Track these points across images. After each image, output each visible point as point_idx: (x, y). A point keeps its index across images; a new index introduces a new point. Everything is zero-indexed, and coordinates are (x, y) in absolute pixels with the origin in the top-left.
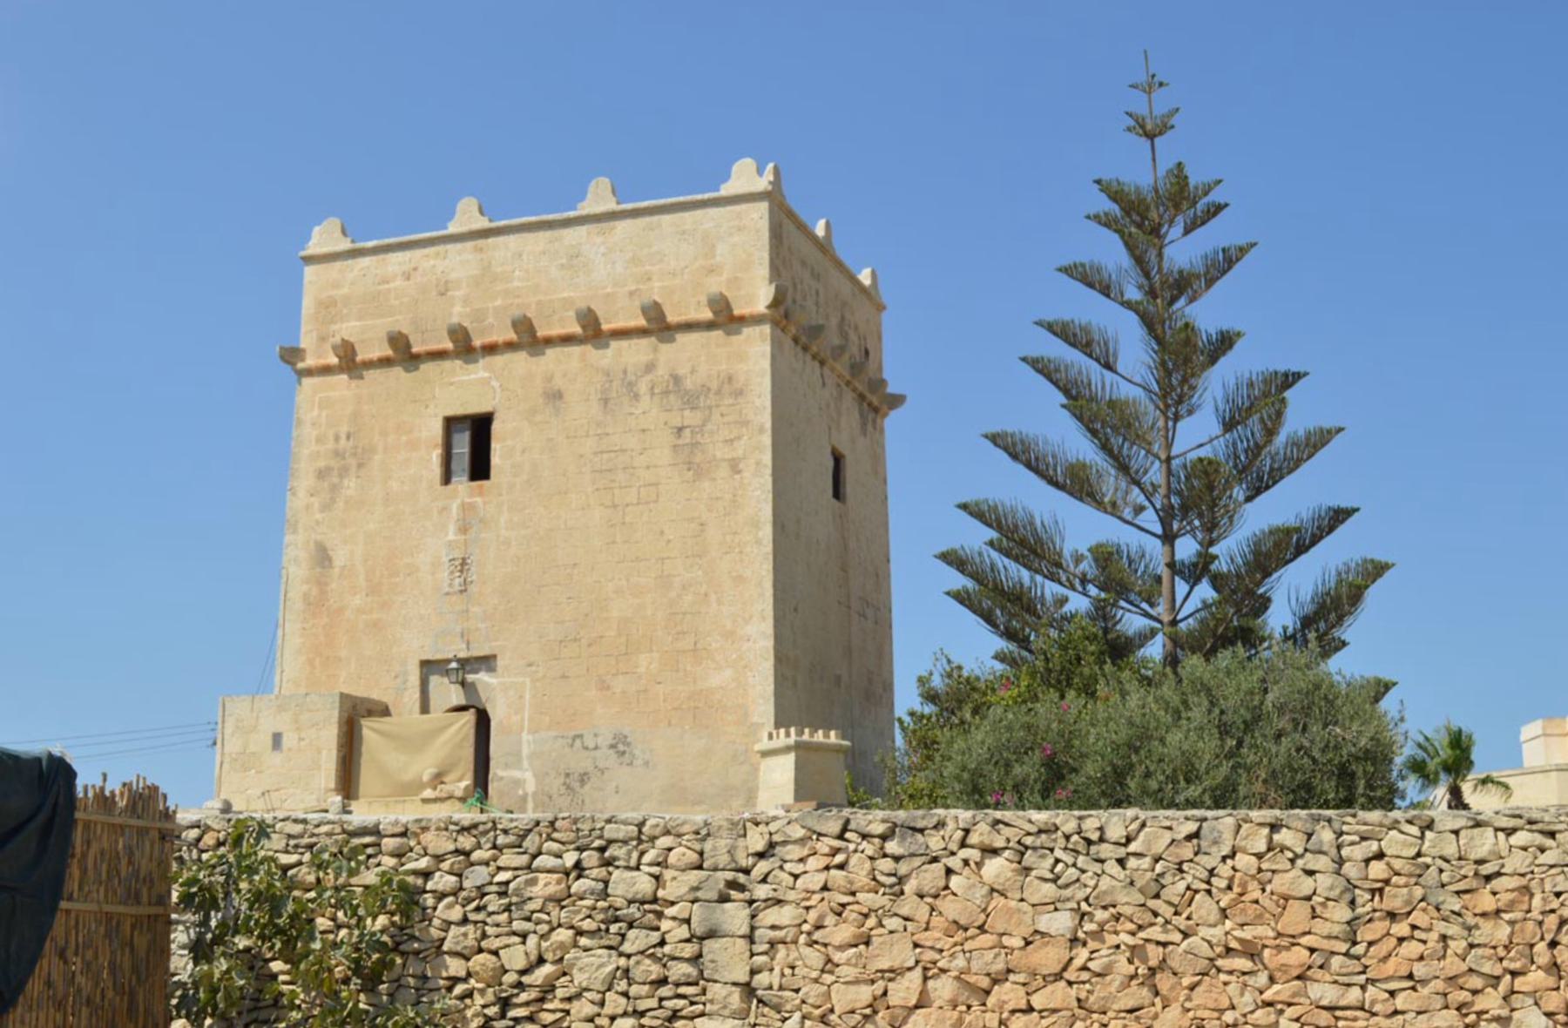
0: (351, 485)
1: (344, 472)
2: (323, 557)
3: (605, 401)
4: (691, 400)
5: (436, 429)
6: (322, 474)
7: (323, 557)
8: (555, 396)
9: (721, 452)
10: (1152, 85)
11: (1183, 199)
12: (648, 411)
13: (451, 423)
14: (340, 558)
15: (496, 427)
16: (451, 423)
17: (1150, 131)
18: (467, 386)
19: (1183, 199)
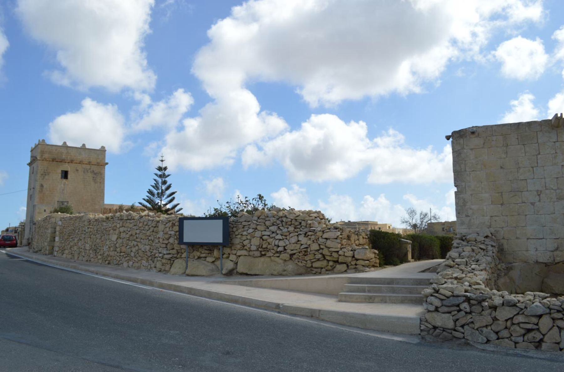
0: (47, 177)
1: (45, 175)
2: (42, 186)
3: (84, 172)
4: (95, 174)
5: (60, 172)
6: (42, 175)
7: (42, 186)
8: (77, 170)
9: (98, 181)
10: (162, 157)
11: (165, 169)
12: (90, 175)
13: (62, 171)
14: (45, 186)
15: (69, 173)
16: (62, 171)
17: (162, 161)
18: (66, 167)
19: (165, 169)
